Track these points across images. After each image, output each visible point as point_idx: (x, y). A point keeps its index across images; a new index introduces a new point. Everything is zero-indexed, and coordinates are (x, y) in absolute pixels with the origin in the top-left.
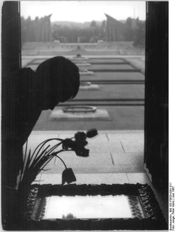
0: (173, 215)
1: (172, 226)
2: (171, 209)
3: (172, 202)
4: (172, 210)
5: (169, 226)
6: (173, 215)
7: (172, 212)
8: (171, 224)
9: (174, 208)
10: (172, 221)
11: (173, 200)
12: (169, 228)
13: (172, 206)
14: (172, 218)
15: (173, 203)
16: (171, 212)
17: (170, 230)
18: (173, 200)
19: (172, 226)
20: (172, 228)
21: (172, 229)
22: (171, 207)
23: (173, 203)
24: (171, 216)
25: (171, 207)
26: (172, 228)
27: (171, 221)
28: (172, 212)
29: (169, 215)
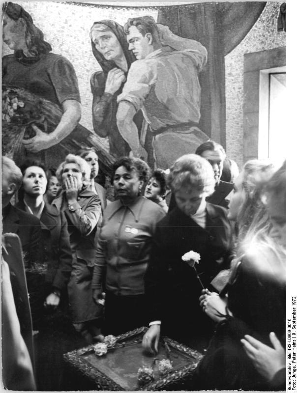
0: (293, 365)
1: (292, 384)
2: (290, 354)
3: (292, 343)
4: (292, 356)
5: (287, 383)
6: (293, 365)
7: (292, 359)
8: (290, 379)
9: (294, 352)
10: (292, 375)
11: (294, 339)
12: (287, 387)
13: (291, 349)
14: (292, 368)
15: (294, 344)
16: (289, 358)
17: (289, 389)
18: (294, 339)
19: (292, 384)
20: (292, 386)
21: (291, 388)
22: (291, 351)
23: (294, 344)
24: (290, 367)
25: (290, 351)
26: (292, 386)
27: (290, 374)
28: (292, 359)
29: (287, 365)
